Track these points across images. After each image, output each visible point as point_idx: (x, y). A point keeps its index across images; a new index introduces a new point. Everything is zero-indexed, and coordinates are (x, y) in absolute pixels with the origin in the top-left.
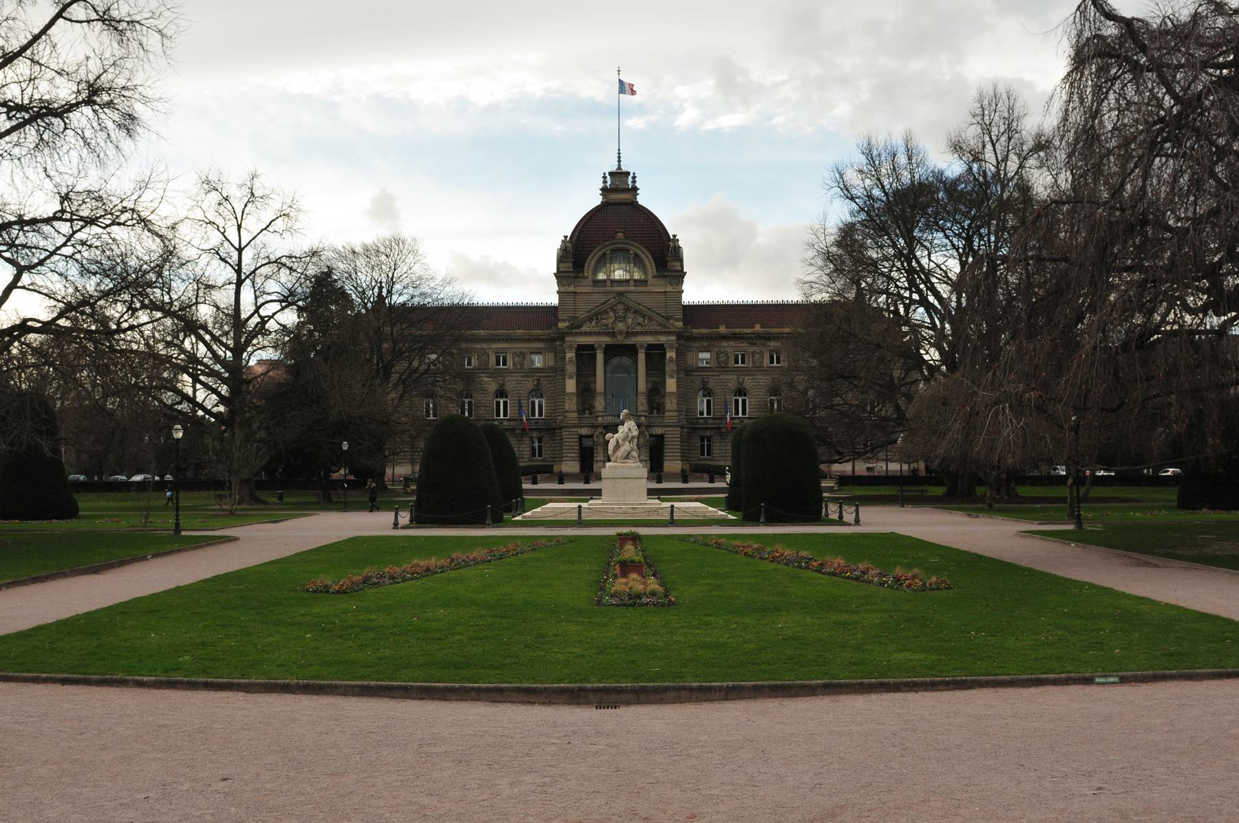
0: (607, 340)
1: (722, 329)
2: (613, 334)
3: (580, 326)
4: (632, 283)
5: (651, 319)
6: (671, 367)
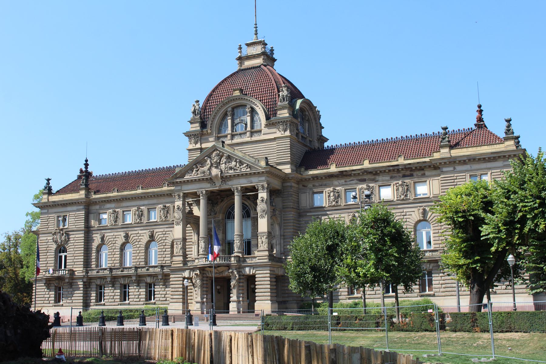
1: (333, 169)
2: (210, 180)
3: (183, 176)
4: (248, 134)
5: (241, 163)
6: (261, 206)
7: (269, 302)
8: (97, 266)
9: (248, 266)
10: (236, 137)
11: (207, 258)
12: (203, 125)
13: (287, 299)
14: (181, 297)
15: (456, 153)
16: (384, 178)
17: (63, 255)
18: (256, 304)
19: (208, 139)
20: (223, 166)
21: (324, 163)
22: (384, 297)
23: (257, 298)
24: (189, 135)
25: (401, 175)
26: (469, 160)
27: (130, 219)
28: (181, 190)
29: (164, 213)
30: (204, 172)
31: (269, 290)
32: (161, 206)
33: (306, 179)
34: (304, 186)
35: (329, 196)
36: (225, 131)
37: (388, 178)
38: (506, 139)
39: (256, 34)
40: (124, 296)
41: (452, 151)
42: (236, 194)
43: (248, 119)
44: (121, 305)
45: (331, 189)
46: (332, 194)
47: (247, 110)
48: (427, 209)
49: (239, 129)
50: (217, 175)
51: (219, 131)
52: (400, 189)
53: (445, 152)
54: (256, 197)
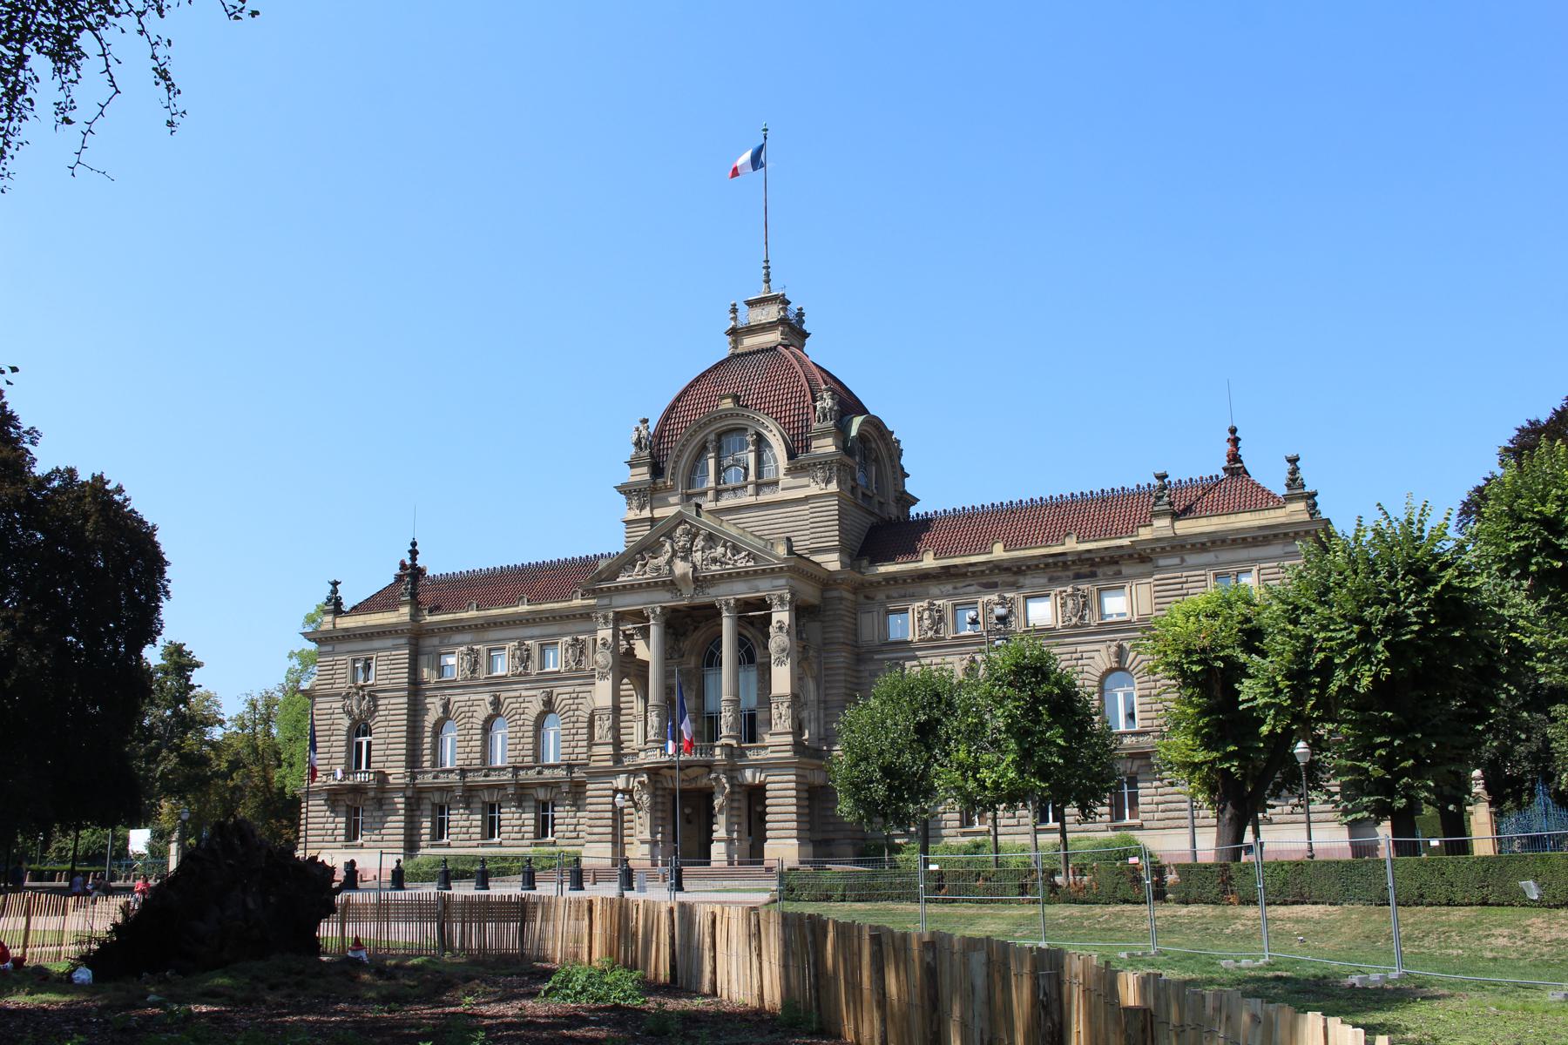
0: (667, 599)
1: (929, 561)
2: (671, 585)
4: (751, 488)
5: (736, 549)
6: (778, 641)
7: (795, 841)
8: (434, 764)
9: (749, 766)
10: (725, 495)
11: (664, 749)
12: (657, 470)
13: (832, 836)
14: (610, 830)
15: (1185, 527)
16: (1036, 581)
17: (364, 740)
18: (766, 846)
19: (666, 499)
20: (698, 556)
21: (911, 551)
22: (1037, 832)
23: (768, 834)
24: (627, 490)
25: (1070, 573)
26: (1213, 542)
27: (502, 667)
28: (609, 606)
29: (574, 654)
30: (658, 569)
31: (794, 817)
32: (568, 639)
33: (871, 584)
34: (867, 597)
35: (921, 619)
36: (702, 482)
37: (1044, 581)
38: (1289, 499)
39: (767, 281)
40: (490, 828)
41: (1178, 524)
42: (725, 614)
43: (751, 458)
44: (483, 845)
45: (925, 604)
46: (926, 615)
47: (750, 439)
48: (1127, 645)
49: (732, 478)
50: (685, 575)
51: (690, 483)
52: (1070, 603)
53: (1162, 527)
54: (767, 620)
